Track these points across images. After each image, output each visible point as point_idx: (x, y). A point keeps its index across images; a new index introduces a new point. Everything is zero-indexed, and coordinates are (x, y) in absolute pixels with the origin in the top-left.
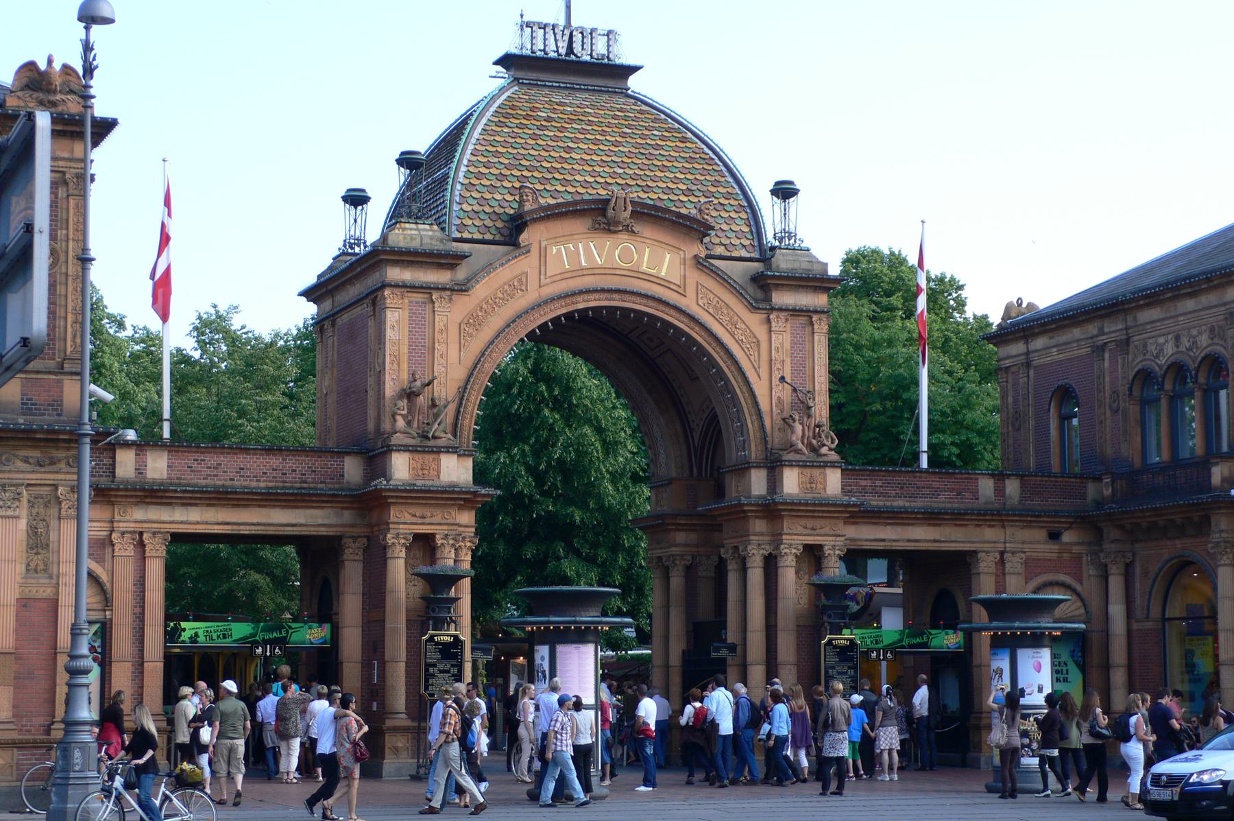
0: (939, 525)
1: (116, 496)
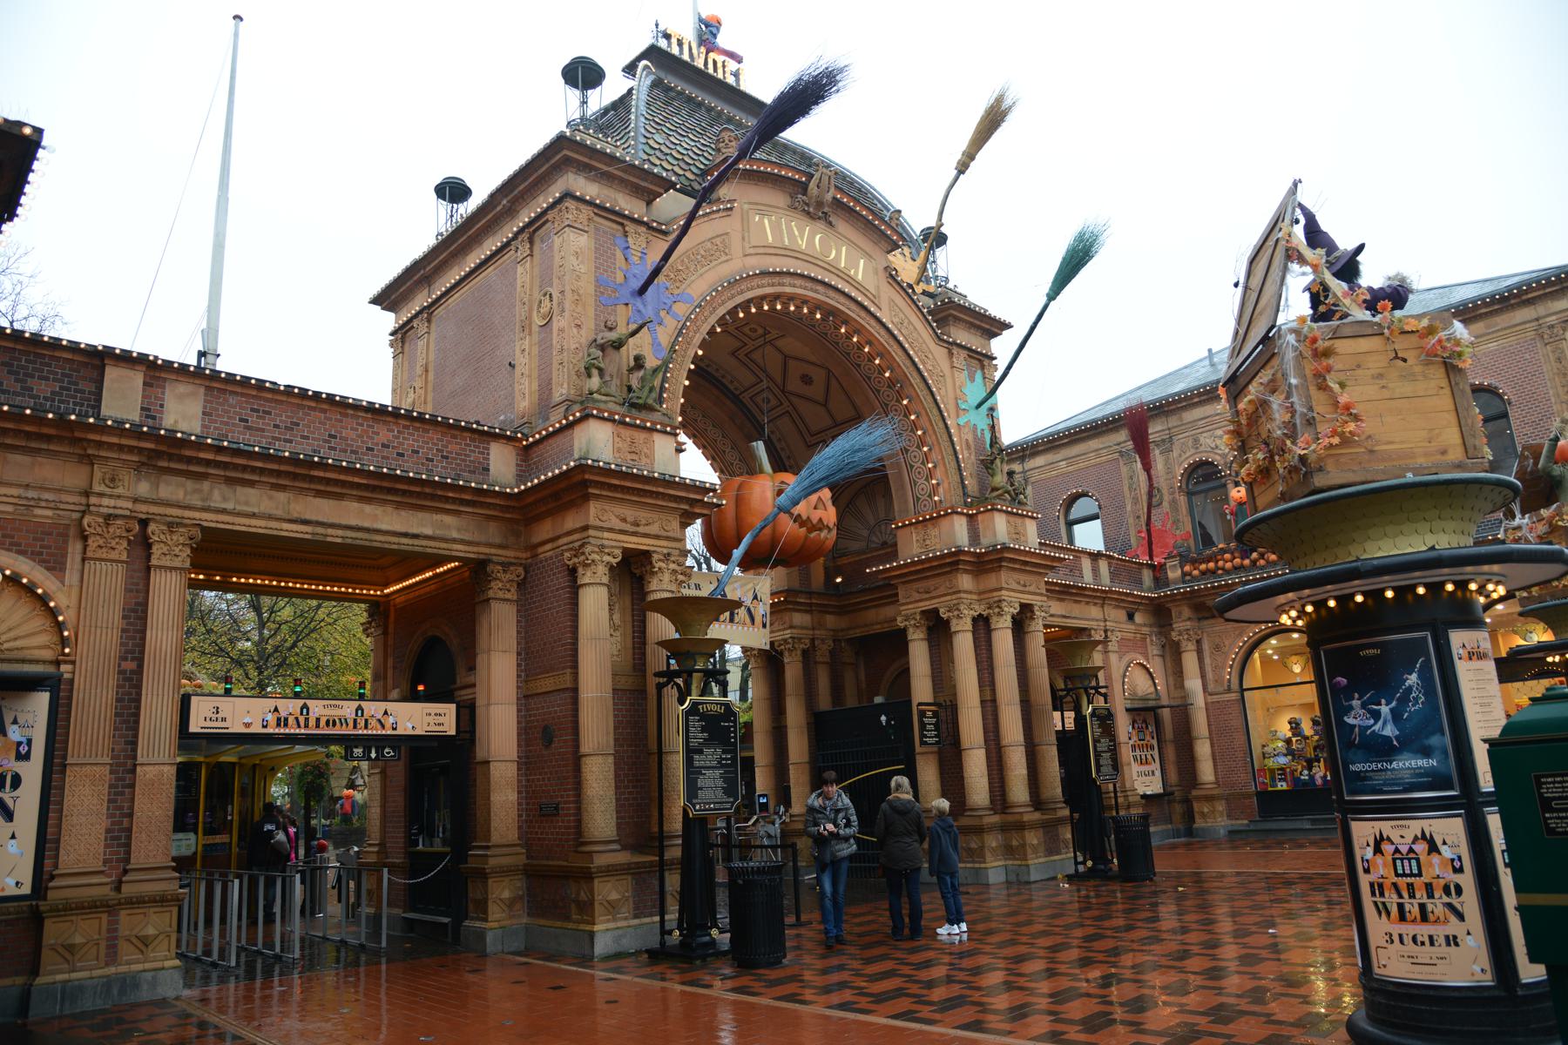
1: (100, 444)
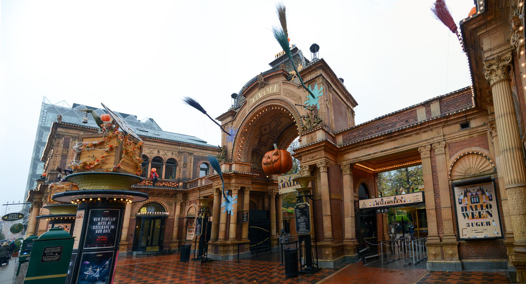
0: (396, 140)
